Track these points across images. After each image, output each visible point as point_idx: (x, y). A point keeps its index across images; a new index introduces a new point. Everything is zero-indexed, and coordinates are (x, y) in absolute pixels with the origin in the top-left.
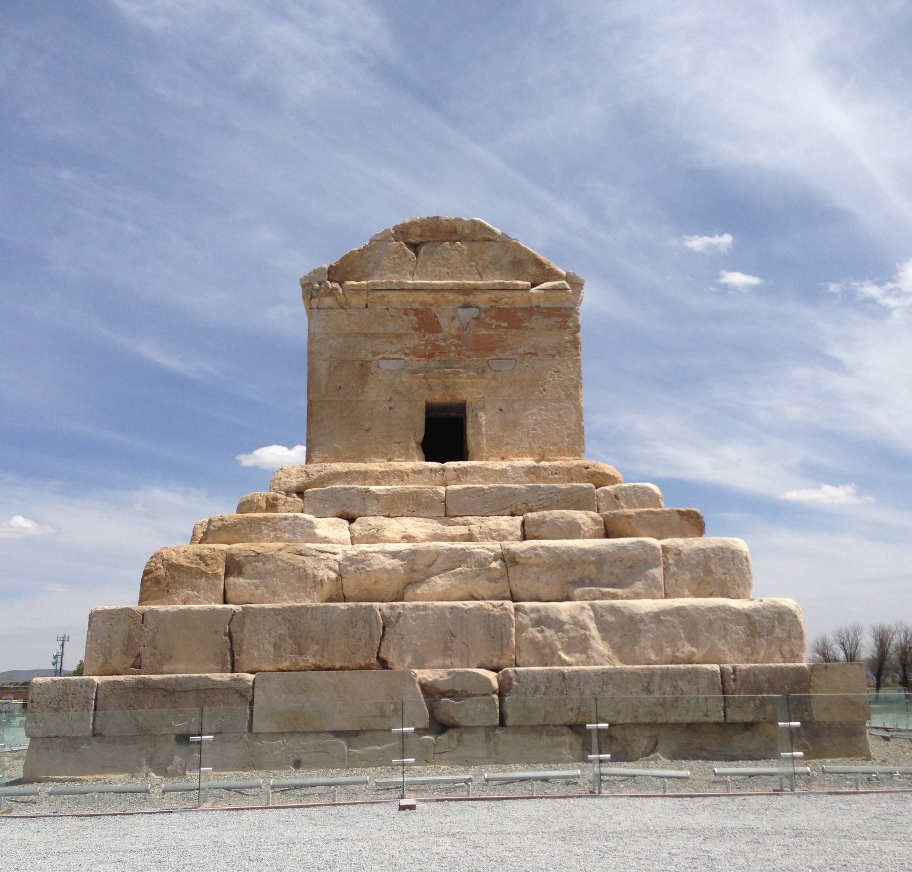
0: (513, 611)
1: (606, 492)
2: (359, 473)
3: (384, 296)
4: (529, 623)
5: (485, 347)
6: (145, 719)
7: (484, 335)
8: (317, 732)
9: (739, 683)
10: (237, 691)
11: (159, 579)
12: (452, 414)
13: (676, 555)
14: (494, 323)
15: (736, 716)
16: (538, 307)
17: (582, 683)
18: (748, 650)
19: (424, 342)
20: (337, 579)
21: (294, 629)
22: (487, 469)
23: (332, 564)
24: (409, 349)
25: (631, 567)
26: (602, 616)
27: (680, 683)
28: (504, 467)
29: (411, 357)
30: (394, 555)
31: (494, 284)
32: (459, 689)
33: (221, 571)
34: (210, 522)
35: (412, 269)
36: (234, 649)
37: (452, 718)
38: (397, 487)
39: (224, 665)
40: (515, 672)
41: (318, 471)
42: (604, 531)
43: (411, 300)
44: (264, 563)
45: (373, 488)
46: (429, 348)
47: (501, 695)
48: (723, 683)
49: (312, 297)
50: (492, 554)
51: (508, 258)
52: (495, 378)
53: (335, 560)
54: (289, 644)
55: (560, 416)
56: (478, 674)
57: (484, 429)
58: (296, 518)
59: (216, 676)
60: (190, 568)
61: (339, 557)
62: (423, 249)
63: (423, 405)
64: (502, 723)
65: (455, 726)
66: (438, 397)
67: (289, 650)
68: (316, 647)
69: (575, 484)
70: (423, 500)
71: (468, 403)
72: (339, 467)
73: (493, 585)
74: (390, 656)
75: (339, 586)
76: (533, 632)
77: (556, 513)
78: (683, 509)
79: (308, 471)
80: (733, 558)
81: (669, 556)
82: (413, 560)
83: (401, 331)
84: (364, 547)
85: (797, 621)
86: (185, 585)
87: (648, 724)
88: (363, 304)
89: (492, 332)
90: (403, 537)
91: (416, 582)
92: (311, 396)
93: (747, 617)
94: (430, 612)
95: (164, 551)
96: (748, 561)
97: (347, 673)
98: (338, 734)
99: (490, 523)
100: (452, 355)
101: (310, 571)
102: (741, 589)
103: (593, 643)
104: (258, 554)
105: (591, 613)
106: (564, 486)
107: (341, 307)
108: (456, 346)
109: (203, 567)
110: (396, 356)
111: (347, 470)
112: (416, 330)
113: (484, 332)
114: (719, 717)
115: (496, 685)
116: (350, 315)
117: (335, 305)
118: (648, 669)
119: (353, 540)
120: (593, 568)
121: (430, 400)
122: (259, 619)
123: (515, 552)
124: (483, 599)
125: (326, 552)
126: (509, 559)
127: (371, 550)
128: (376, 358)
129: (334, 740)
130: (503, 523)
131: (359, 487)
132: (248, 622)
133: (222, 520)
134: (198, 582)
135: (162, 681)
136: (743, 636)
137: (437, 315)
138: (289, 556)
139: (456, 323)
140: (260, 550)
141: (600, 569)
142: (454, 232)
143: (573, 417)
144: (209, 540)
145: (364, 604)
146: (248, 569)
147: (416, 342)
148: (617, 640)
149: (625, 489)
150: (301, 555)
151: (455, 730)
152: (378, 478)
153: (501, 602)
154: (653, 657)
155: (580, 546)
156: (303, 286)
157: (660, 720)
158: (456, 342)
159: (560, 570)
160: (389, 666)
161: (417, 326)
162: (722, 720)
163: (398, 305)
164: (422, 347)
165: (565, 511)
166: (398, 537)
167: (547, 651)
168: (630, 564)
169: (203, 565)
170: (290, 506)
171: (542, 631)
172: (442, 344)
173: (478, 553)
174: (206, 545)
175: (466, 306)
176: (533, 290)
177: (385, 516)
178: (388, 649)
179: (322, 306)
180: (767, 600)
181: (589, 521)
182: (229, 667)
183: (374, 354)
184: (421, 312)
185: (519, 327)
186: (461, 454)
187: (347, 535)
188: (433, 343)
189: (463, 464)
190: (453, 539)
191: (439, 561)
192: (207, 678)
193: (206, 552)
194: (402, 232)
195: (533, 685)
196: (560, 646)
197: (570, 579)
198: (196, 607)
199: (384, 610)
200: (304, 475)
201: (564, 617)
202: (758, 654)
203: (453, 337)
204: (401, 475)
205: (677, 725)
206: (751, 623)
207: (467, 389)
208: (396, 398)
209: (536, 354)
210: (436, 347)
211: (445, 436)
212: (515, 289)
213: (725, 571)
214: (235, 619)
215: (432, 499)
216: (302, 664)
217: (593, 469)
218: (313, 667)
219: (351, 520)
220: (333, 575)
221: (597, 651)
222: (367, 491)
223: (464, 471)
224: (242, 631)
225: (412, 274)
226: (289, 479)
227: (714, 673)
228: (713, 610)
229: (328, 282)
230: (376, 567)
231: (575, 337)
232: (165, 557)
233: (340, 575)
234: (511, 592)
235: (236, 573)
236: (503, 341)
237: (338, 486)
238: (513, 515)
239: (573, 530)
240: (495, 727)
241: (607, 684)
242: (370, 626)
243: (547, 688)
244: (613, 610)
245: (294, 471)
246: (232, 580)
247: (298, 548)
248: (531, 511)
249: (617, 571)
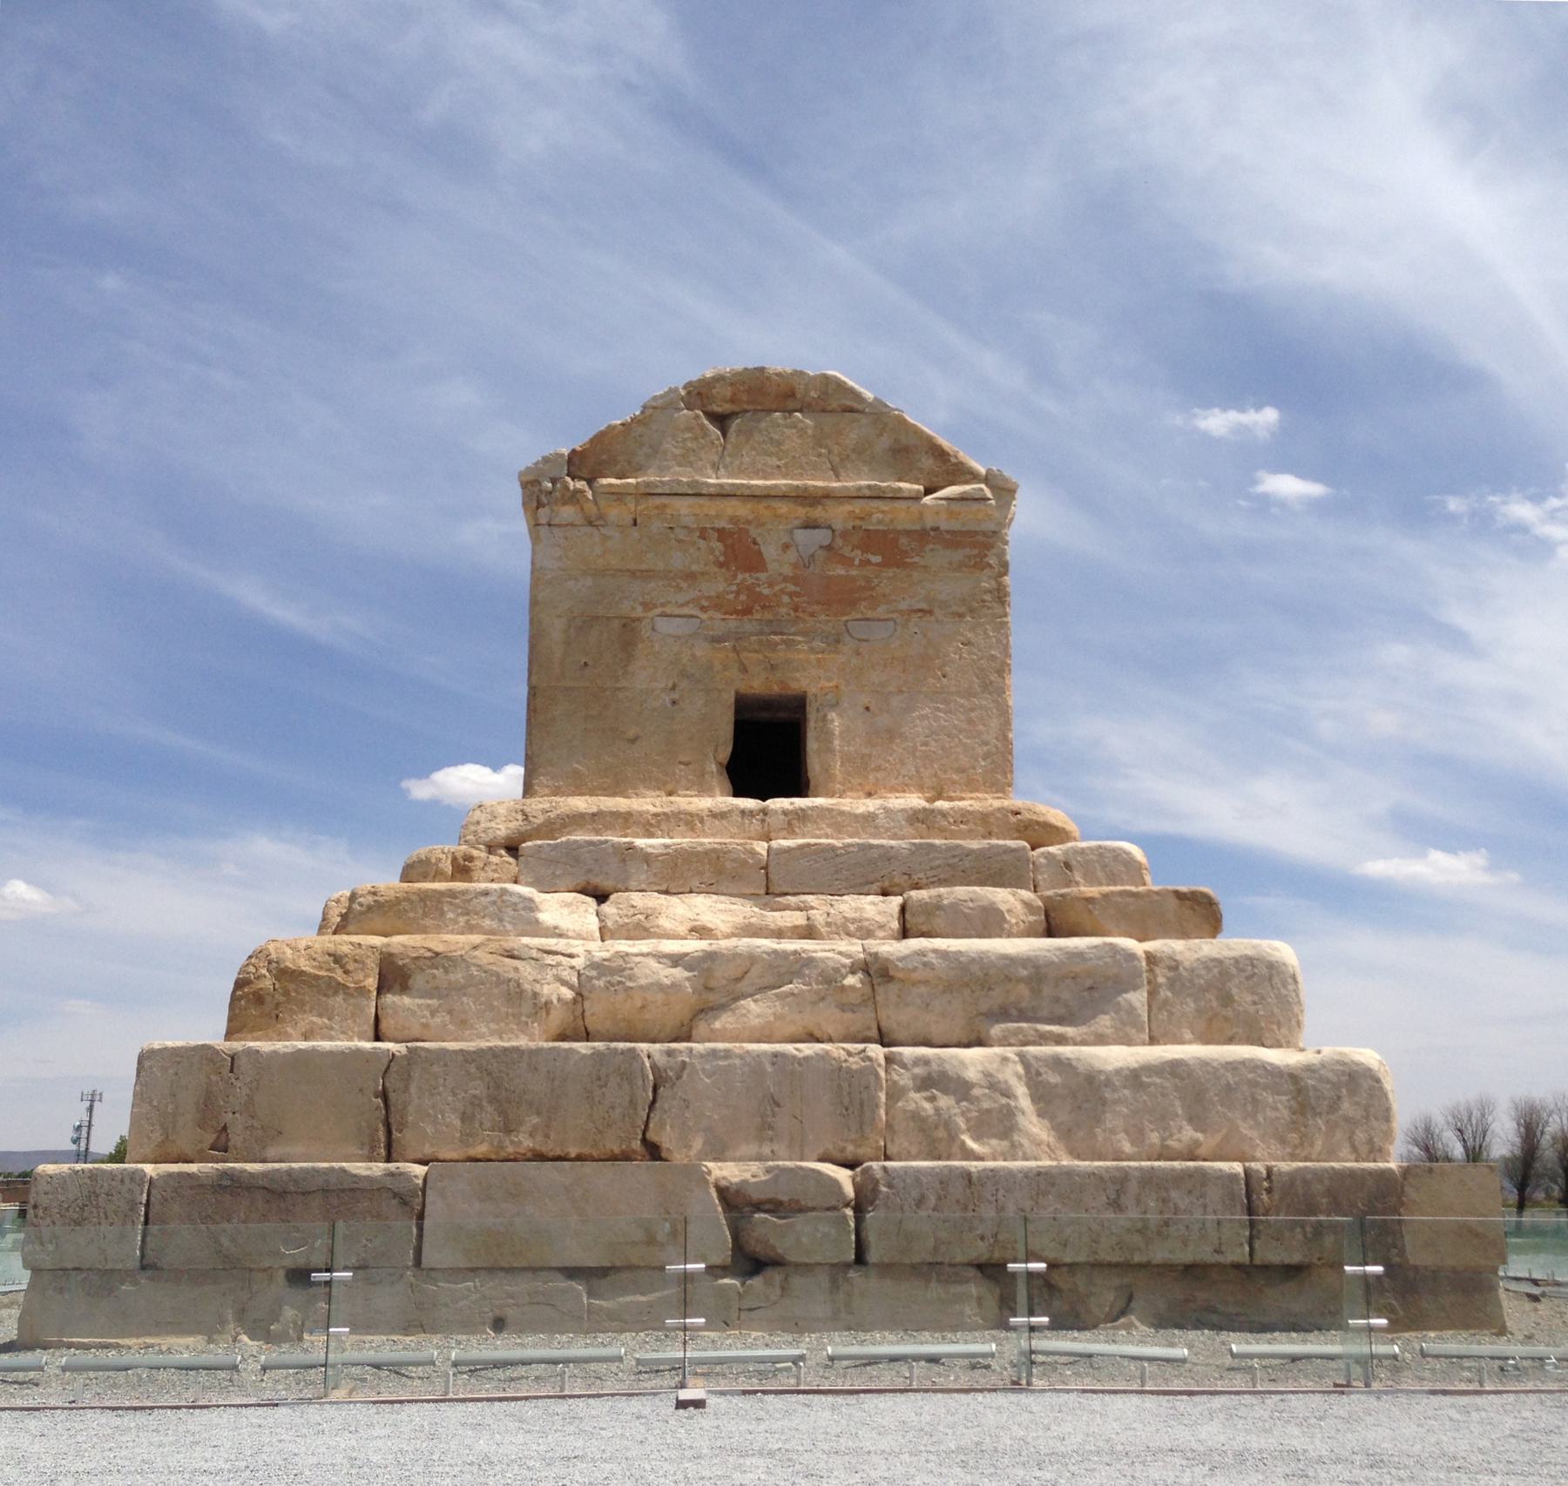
0: (883, 1062)
1: (1049, 856)
2: (616, 815)
3: (665, 506)
4: (910, 1083)
5: (842, 598)
6: (233, 1240)
7: (840, 576)
8: (534, 1270)
9: (1276, 1197)
10: (395, 1195)
11: (261, 995)
12: (782, 715)
13: (1170, 968)
14: (857, 555)
15: (1271, 1254)
16: (936, 529)
17: (1001, 1192)
18: (1293, 1137)
19: (734, 588)
20: (575, 1001)
21: (498, 1087)
22: (842, 813)
23: (565, 974)
24: (708, 598)
25: (1091, 988)
26: (1039, 1074)
27: (1174, 1194)
28: (871, 809)
29: (710, 613)
30: (676, 960)
31: (860, 488)
32: (785, 1198)
33: (371, 982)
34: (353, 897)
35: (716, 458)
36: (392, 1121)
37: (773, 1248)
38: (683, 841)
39: (373, 1149)
40: (885, 1169)
41: (545, 811)
42: (1044, 925)
43: (713, 513)
44: (446, 972)
45: (640, 842)
46: (743, 597)
47: (859, 1209)
48: (1248, 1195)
49: (540, 505)
50: (848, 961)
51: (885, 442)
52: (858, 654)
53: (572, 968)
54: (489, 1114)
55: (970, 721)
56: (819, 1172)
57: (837, 742)
58: (504, 892)
59: (359, 1168)
60: (317, 977)
61: (579, 963)
62: (735, 424)
63: (730, 698)
64: (860, 1259)
65: (777, 1263)
66: (759, 684)
67: (487, 1125)
68: (535, 1120)
69: (994, 841)
70: (728, 865)
71: (810, 695)
72: (581, 804)
73: (848, 1015)
74: (665, 1138)
75: (578, 1013)
76: (917, 1101)
77: (961, 891)
78: (1183, 889)
79: (527, 810)
80: (1270, 979)
81: (1158, 970)
82: (709, 970)
83: (695, 568)
84: (623, 946)
85: (1381, 1089)
86: (307, 1008)
87: (1117, 1265)
88: (628, 520)
89: (854, 573)
90: (692, 930)
91: (712, 1009)
92: (534, 678)
93: (1293, 1081)
94: (737, 1061)
95: (271, 947)
96: (1296, 982)
97: (589, 1167)
98: (571, 1273)
99: (843, 907)
100: (783, 610)
101: (527, 986)
102: (1284, 1031)
103: (1021, 1120)
104: (437, 954)
105: (1020, 1069)
106: (975, 844)
107: (590, 524)
108: (791, 595)
109: (339, 975)
110: (686, 611)
111: (595, 809)
112: (721, 565)
113: (840, 571)
114: (1240, 1254)
115: (849, 1191)
116: (605, 538)
117: (579, 520)
118: (1118, 1169)
119: (604, 933)
120: (1023, 990)
121: (744, 689)
122: (436, 1069)
123: (887, 960)
124: (830, 1040)
125: (556, 953)
126: (876, 971)
127: (635, 950)
128: (650, 614)
129: (563, 1283)
130: (868, 907)
131: (616, 839)
132: (416, 1074)
133: (374, 894)
134: (331, 1001)
135: (265, 1174)
136: (1286, 1113)
138: (491, 958)
139: (792, 556)
140: (440, 948)
141: (1037, 992)
142: (791, 394)
143: (994, 723)
144: (351, 928)
145: (621, 1045)
146: (418, 981)
147: (721, 586)
148: (1063, 1117)
149: (1082, 851)
150: (512, 957)
151: (779, 1269)
152: (649, 825)
153: (860, 1046)
154: (1127, 1147)
155: (1002, 951)
156: (524, 485)
157: (1137, 1258)
158: (791, 588)
159: (967, 992)
160: (664, 1155)
161: (722, 559)
162: (1247, 1259)
163: (688, 521)
164: (731, 597)
165: (977, 889)
166: (682, 930)
167: (941, 1133)
168: (1089, 982)
169: (339, 971)
170: (495, 871)
171: (932, 1099)
172: (766, 591)
173: (823, 960)
174: (345, 937)
175: (810, 525)
176: (927, 499)
177: (660, 892)
178: (662, 1125)
179: (556, 521)
180: (1328, 1051)
181: (1019, 907)
182: (383, 1152)
183: (647, 606)
184: (731, 534)
185: (901, 564)
186: (798, 787)
187: (593, 923)
188: (750, 590)
189: (799, 802)
190: (779, 934)
191: (755, 971)
192: (343, 1170)
193: (346, 949)
194: (698, 394)
195: (915, 1194)
196: (963, 1126)
197: (984, 1007)
198: (326, 1045)
199: (657, 1057)
200: (520, 817)
201: (972, 1074)
202: (1312, 1145)
203: (786, 579)
204: (689, 821)
205: (1167, 1267)
206: (1299, 1091)
207: (808, 671)
208: (684, 684)
209: (931, 612)
210: (756, 597)
211: (768, 753)
212: (896, 497)
213: (1256, 998)
214: (394, 1068)
216: (511, 1149)
217: (1027, 816)
218: (529, 1155)
219: (601, 898)
220: (568, 994)
221: (1028, 1134)
222: (630, 847)
223: (802, 816)
224: (406, 1089)
225: (715, 467)
226: (493, 824)
227: (1233, 1177)
228: (1233, 1066)
229: (568, 479)
230: (643, 982)
231: (999, 584)
232: (273, 956)
233: (579, 994)
234: (879, 1029)
235: (397, 987)
236: (873, 589)
237: (579, 837)
238: (885, 893)
239: (990, 922)
240: (847, 1266)
241: (1045, 1194)
242: (631, 1083)
243: (939, 1198)
244: (1058, 1063)
245: (502, 811)
246: (389, 999)
247: (507, 946)
248: (917, 887)
249: (1066, 995)
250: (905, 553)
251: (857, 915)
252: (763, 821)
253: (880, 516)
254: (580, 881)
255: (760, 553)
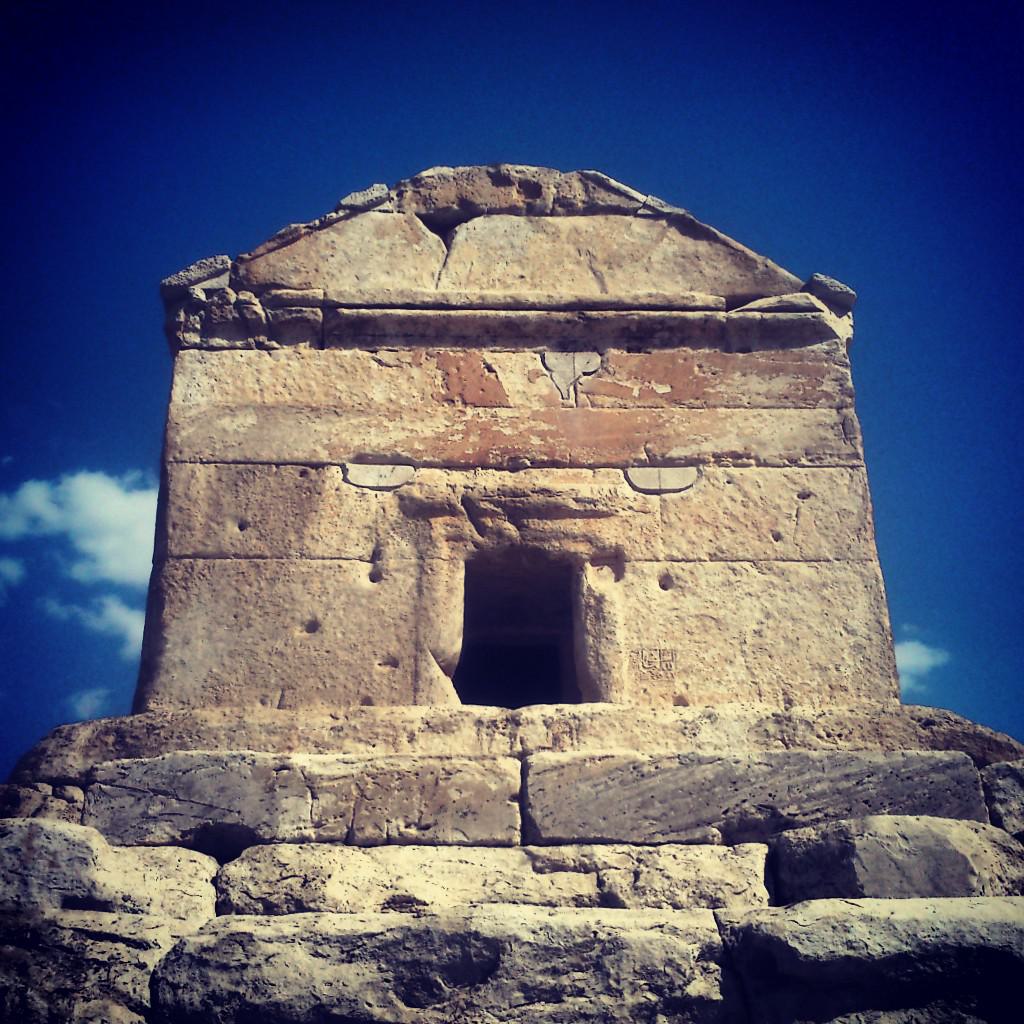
19: (461, 427)
28: (689, 718)
35: (437, 267)
46: (473, 439)
50: (694, 950)
57: (621, 635)
77: (884, 823)
108: (542, 435)
125: (114, 938)
127: (268, 932)
137: (495, 367)
147: (436, 424)
158: (544, 427)
165: (911, 819)
172: (508, 431)
176: (733, 314)
188: (485, 430)
203: (535, 416)
215: (481, 791)
229: (229, 291)
250: (701, 383)
251: (691, 875)
252: (513, 736)
253: (666, 334)
254: (193, 824)
255: (500, 383)
